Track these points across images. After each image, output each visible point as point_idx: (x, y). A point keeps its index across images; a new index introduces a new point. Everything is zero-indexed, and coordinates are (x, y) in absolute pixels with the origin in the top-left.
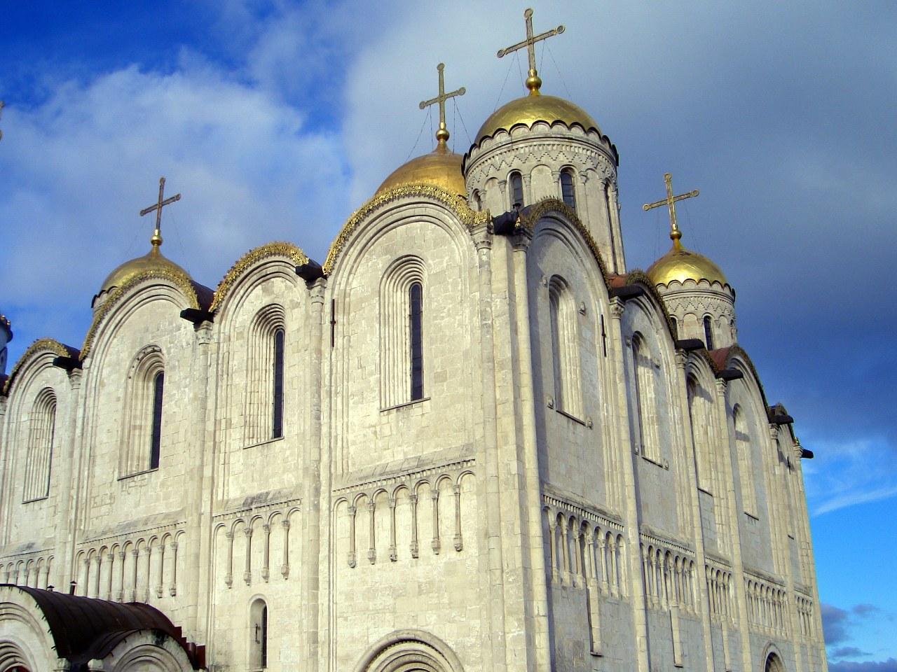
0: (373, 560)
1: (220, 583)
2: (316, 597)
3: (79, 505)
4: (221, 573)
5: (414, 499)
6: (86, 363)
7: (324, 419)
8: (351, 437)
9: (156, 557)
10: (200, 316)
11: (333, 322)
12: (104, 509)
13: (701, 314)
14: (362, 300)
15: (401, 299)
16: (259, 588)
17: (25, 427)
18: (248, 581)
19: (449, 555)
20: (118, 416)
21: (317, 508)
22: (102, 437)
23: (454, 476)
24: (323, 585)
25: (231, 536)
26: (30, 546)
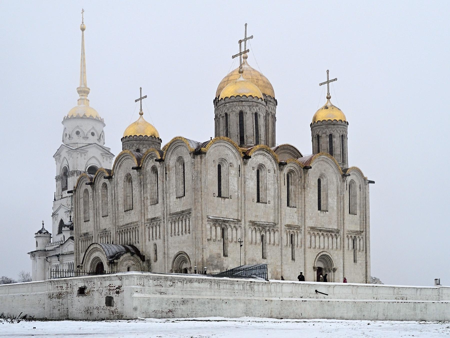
0: (175, 235)
1: (147, 240)
2: (164, 244)
3: (116, 218)
4: (147, 237)
5: (182, 221)
6: (113, 177)
7: (165, 200)
8: (171, 204)
9: (134, 233)
10: (138, 168)
11: (166, 173)
12: (122, 219)
13: (328, 134)
14: (173, 167)
15: (181, 167)
16: (155, 241)
17: (100, 194)
18: (153, 240)
19: (188, 234)
20: (123, 193)
21: (164, 222)
22: (120, 199)
23: (188, 216)
24: (166, 241)
25: (149, 228)
26: (105, 229)
